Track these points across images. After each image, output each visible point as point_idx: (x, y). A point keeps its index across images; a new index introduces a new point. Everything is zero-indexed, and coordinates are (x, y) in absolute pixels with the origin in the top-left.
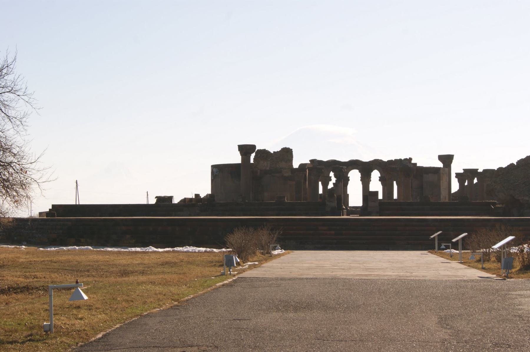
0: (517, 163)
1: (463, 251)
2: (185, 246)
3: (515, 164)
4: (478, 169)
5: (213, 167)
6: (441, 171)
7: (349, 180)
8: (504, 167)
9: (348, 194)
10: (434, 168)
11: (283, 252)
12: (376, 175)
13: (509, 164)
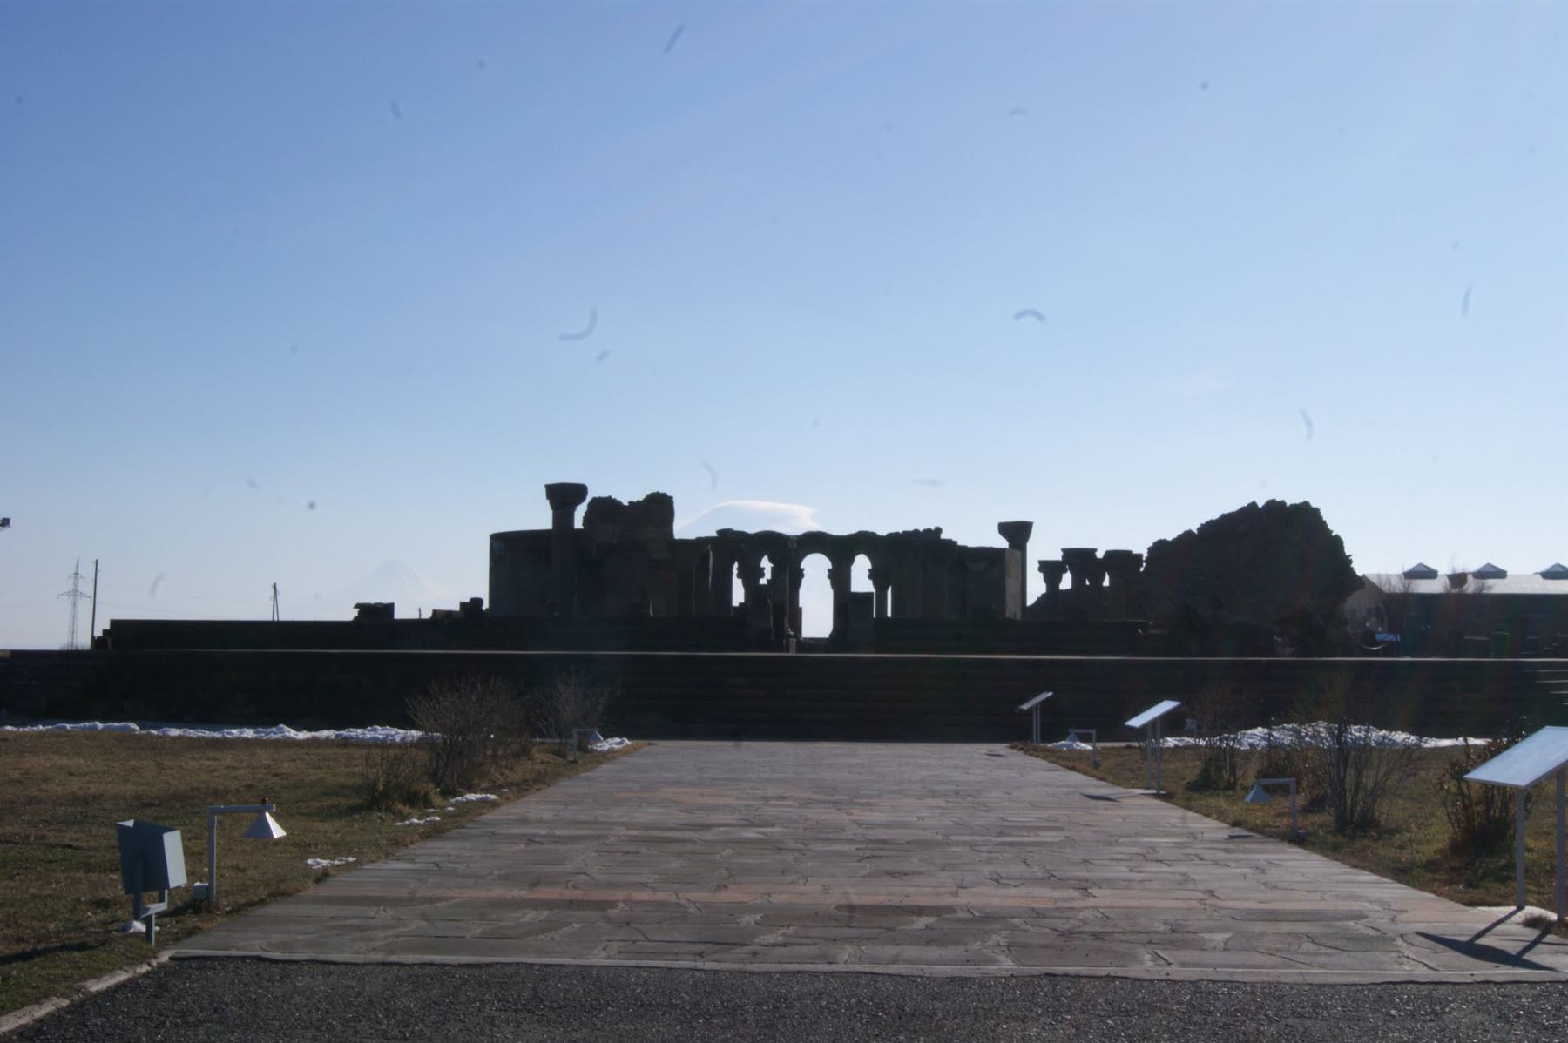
0: (1199, 529)
1: (1100, 745)
2: (371, 726)
3: (1196, 532)
4: (1095, 550)
7: (803, 576)
9: (801, 609)
11: (625, 744)
12: (861, 566)
13: (1181, 532)
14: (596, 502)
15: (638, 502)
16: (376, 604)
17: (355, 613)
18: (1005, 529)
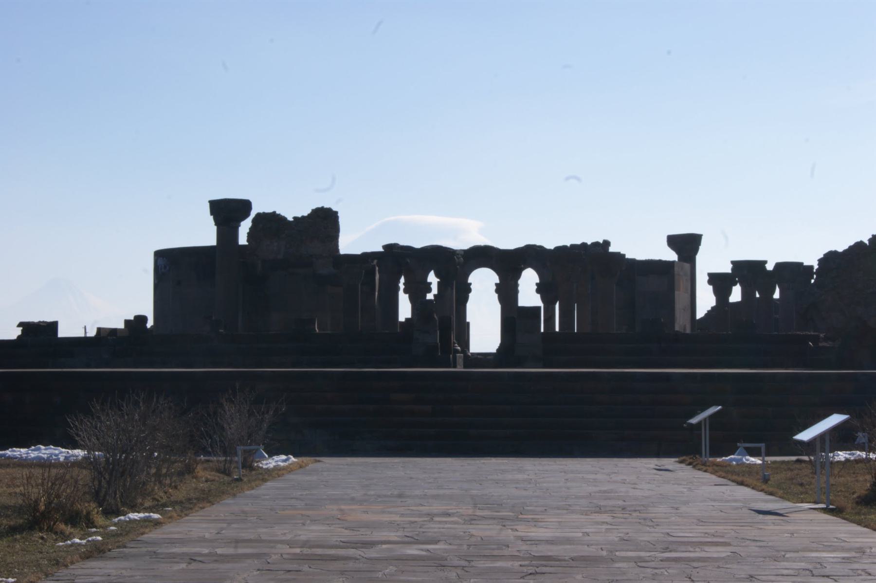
0: (870, 240)
1: (770, 459)
2: (35, 446)
3: (867, 242)
4: (765, 262)
5: (160, 255)
6: (676, 269)
7: (470, 290)
8: (840, 249)
10: (660, 262)
11: (290, 462)
13: (852, 243)
14: (261, 218)
15: (303, 217)
16: (40, 322)
17: (18, 332)
18: (674, 241)
